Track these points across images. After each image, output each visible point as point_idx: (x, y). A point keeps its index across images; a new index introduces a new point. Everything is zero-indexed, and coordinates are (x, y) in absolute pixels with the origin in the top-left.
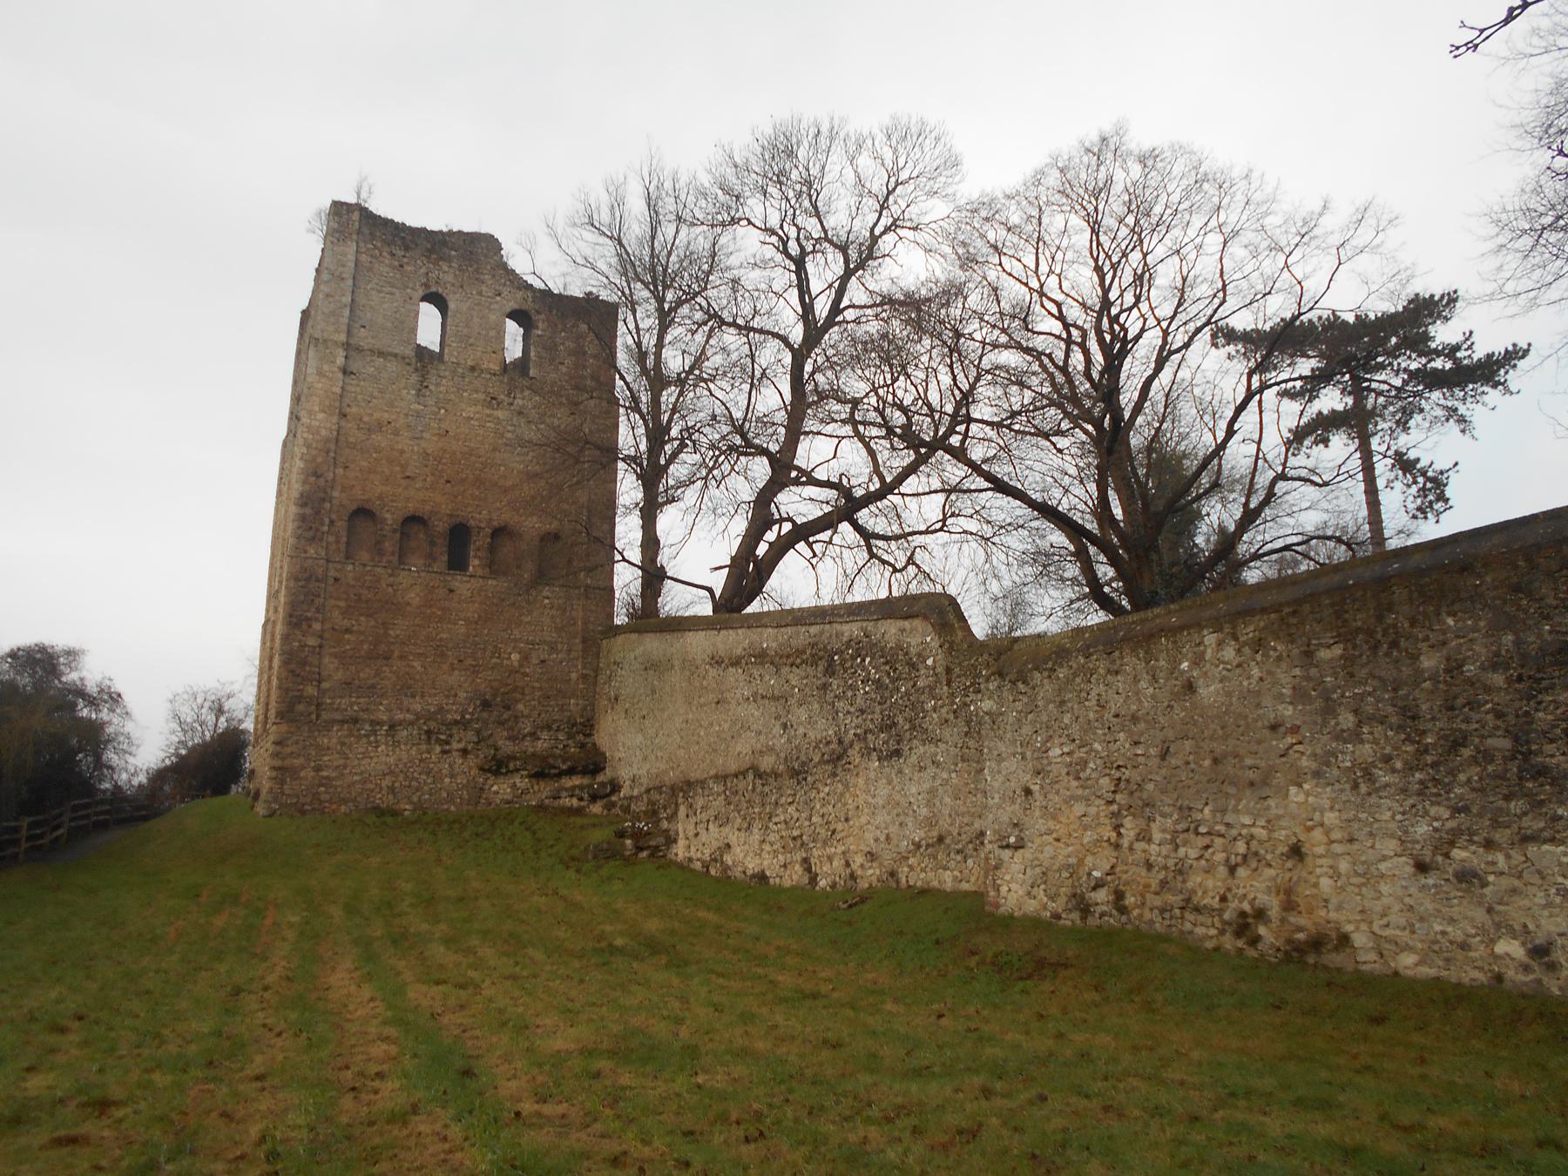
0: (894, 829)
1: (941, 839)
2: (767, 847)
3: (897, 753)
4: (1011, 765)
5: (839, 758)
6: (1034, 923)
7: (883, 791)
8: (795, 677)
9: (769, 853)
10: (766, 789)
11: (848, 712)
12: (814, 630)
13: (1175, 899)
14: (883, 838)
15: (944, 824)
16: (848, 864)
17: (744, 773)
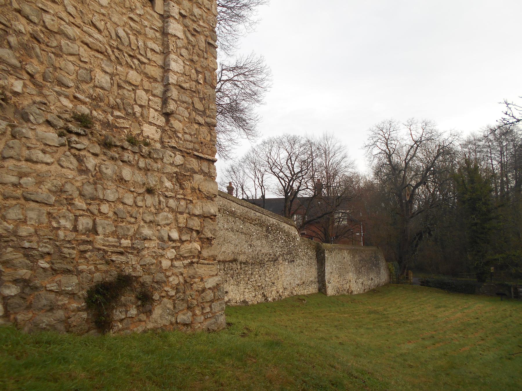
0: (292, 281)
1: (304, 283)
2: (247, 290)
3: (293, 261)
4: (329, 268)
5: (275, 260)
6: (333, 296)
7: (289, 271)
8: (253, 228)
9: (248, 293)
10: (247, 268)
11: (277, 246)
12: (258, 214)
13: (343, 289)
14: (289, 283)
15: (304, 278)
16: (278, 292)
17: (235, 260)
